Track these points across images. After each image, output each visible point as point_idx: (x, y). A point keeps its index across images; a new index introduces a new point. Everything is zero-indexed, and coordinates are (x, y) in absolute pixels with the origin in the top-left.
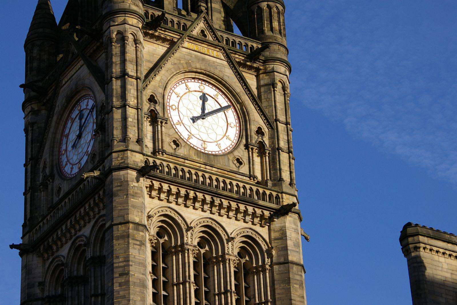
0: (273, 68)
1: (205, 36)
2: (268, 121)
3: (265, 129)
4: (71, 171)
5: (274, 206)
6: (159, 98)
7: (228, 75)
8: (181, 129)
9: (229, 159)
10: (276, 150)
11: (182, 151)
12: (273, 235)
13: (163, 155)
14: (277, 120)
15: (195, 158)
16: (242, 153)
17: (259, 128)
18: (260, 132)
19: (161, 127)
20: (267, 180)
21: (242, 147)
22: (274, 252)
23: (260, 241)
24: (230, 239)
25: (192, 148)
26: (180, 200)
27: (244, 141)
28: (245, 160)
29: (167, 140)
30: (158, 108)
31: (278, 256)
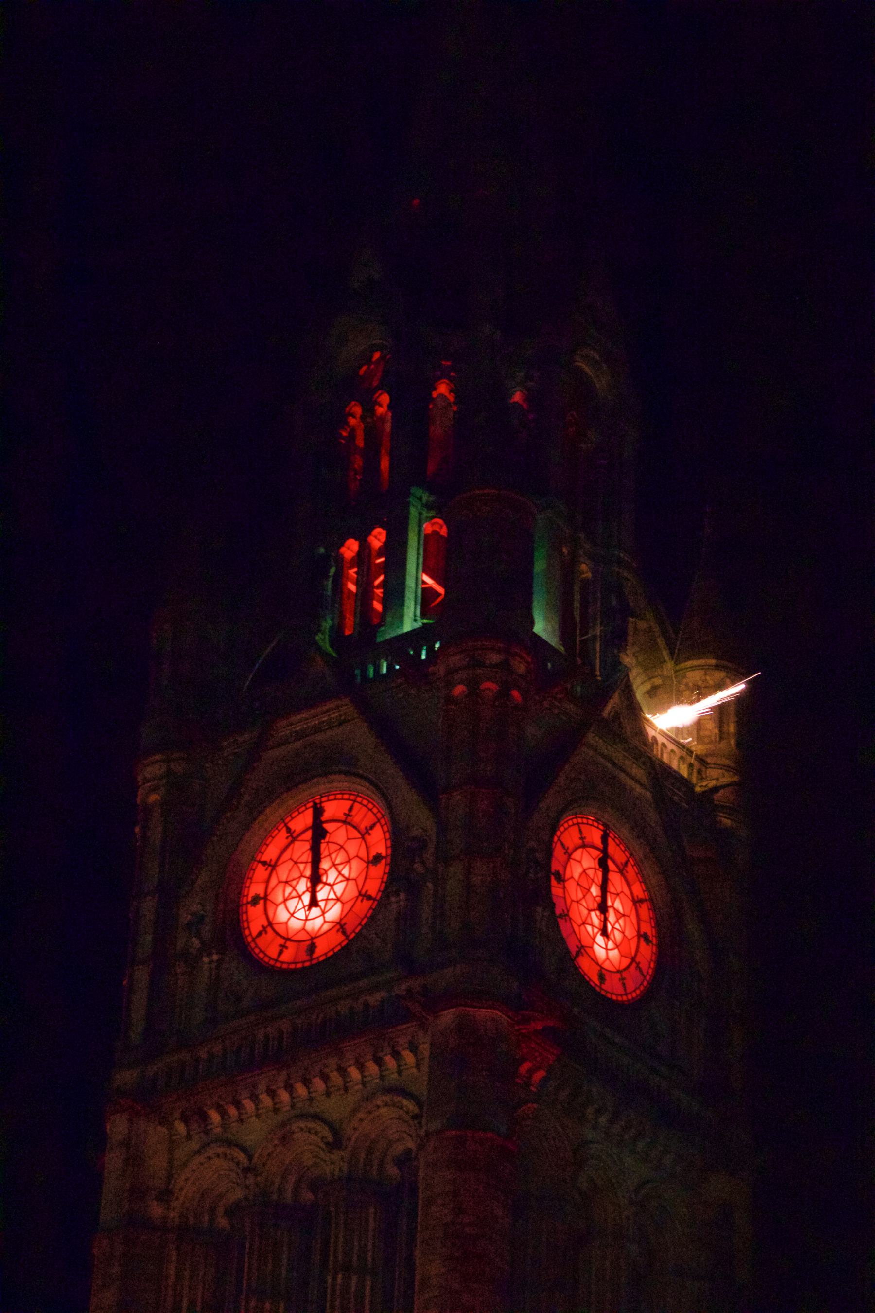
25: (582, 978)
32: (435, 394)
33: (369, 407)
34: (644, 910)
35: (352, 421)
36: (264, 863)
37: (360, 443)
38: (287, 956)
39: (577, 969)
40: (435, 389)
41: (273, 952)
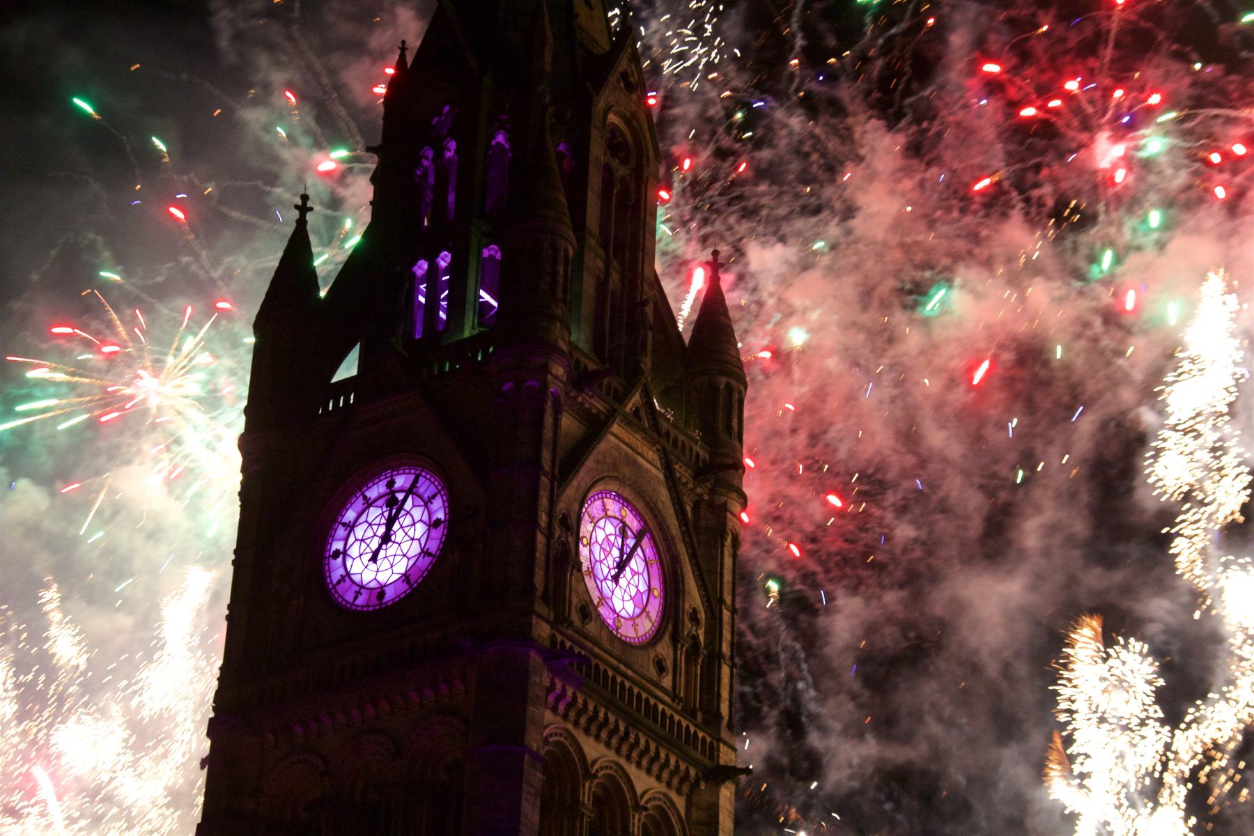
0: (725, 503)
1: (640, 419)
2: (709, 601)
3: (702, 615)
5: (706, 761)
7: (663, 499)
8: (589, 582)
10: (715, 657)
11: (591, 628)
12: (696, 815)
14: (721, 601)
15: (607, 645)
16: (664, 649)
17: (695, 611)
18: (694, 617)
21: (667, 638)
24: (639, 808)
25: (603, 623)
26: (583, 721)
28: (669, 664)
29: (575, 601)
30: (571, 539)
33: (440, 151)
35: (425, 163)
36: (344, 524)
37: (431, 180)
39: (599, 615)
40: (494, 138)
41: (349, 597)
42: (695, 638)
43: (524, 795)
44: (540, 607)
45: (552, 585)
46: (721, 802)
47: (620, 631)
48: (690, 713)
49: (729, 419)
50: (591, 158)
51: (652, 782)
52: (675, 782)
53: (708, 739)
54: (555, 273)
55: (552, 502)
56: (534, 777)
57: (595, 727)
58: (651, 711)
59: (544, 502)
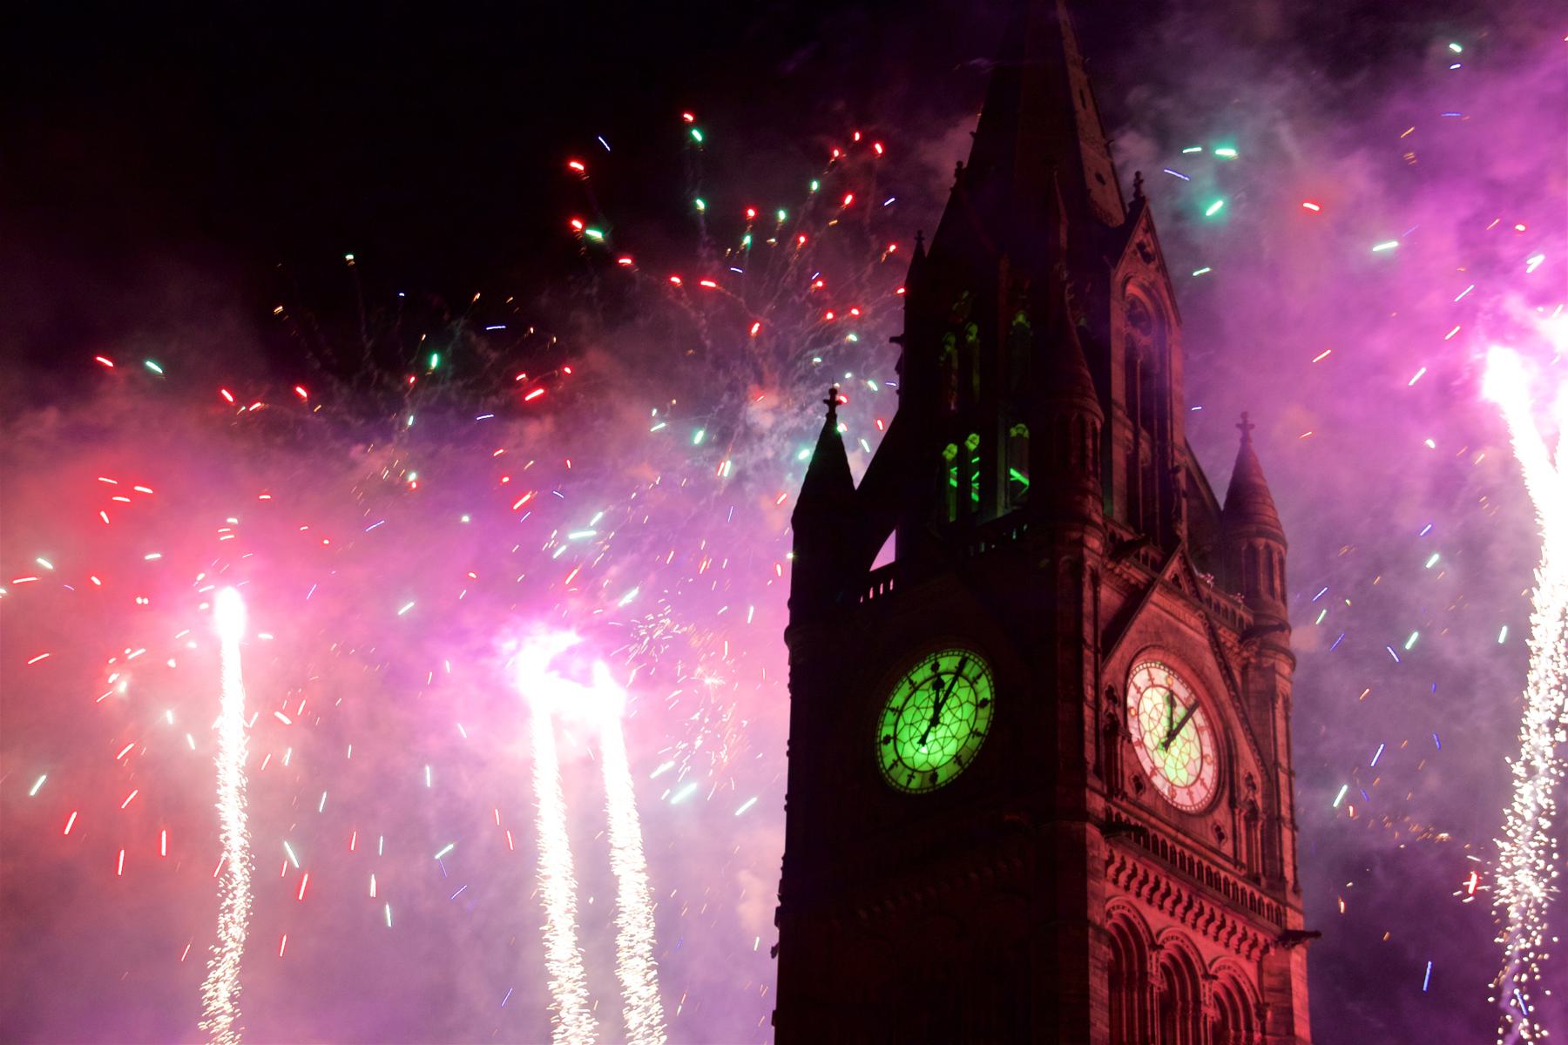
0: (1273, 666)
1: (1180, 586)
2: (1263, 764)
3: (1258, 780)
4: (909, 781)
6: (1120, 693)
7: (1210, 665)
9: (1207, 825)
11: (1146, 798)
12: (1267, 981)
13: (1122, 799)
14: (1276, 764)
15: (1161, 812)
16: (1222, 815)
17: (1250, 777)
19: (1122, 746)
20: (1258, 873)
22: (1269, 1015)
23: (1245, 987)
26: (1145, 890)
27: (1226, 794)
28: (1228, 831)
29: (1127, 772)
30: (1119, 711)
31: (1275, 1022)
32: (1014, 323)
33: (961, 334)
34: (1206, 737)
35: (948, 349)
36: (893, 710)
37: (955, 364)
38: (914, 784)
39: (1153, 785)
40: (1015, 318)
41: (903, 780)
42: (1253, 803)
43: (1091, 969)
44: (1093, 781)
45: (1103, 757)
46: (1293, 966)
47: (1175, 800)
48: (1255, 880)
49: (1271, 580)
50: (1113, 329)
51: (1218, 948)
52: (1245, 947)
53: (1274, 904)
54: (1084, 447)
55: (1097, 675)
56: (1101, 952)
57: (1157, 896)
58: (1213, 880)
59: (1089, 675)
